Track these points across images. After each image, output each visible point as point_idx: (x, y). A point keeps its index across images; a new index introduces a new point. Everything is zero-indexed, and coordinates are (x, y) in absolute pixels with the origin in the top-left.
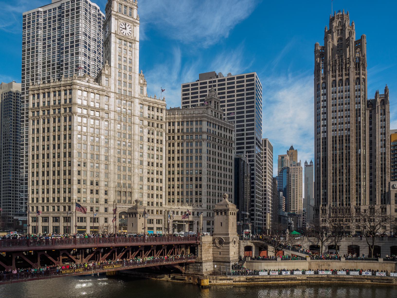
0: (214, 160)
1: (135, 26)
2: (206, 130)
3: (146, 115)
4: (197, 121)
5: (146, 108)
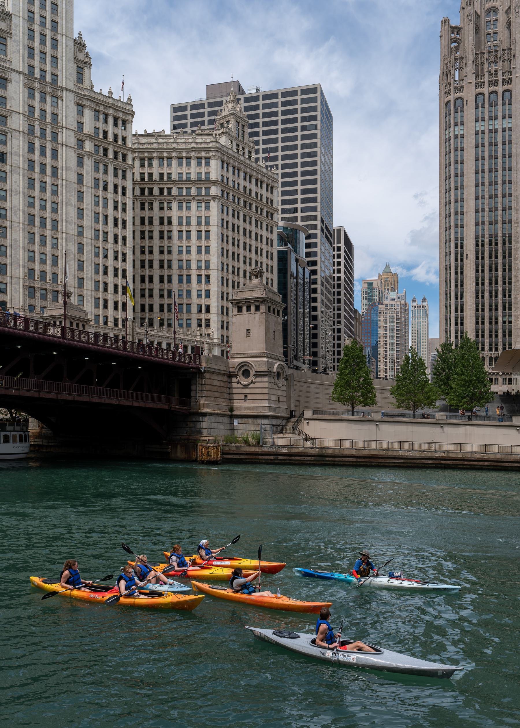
2: (219, 178)
4: (201, 158)
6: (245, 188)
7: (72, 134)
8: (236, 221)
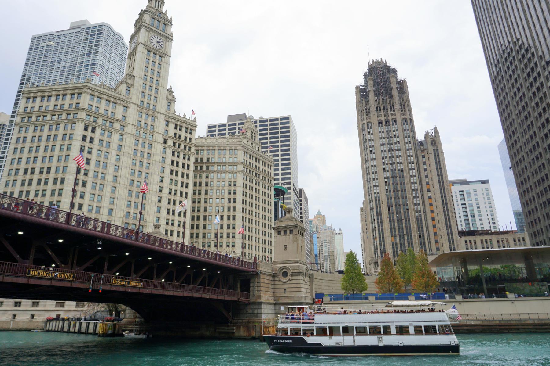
0: (251, 196)
1: (168, 41)
2: (243, 161)
3: (171, 133)
5: (172, 126)
6: (256, 166)
7: (161, 136)
8: (251, 184)
